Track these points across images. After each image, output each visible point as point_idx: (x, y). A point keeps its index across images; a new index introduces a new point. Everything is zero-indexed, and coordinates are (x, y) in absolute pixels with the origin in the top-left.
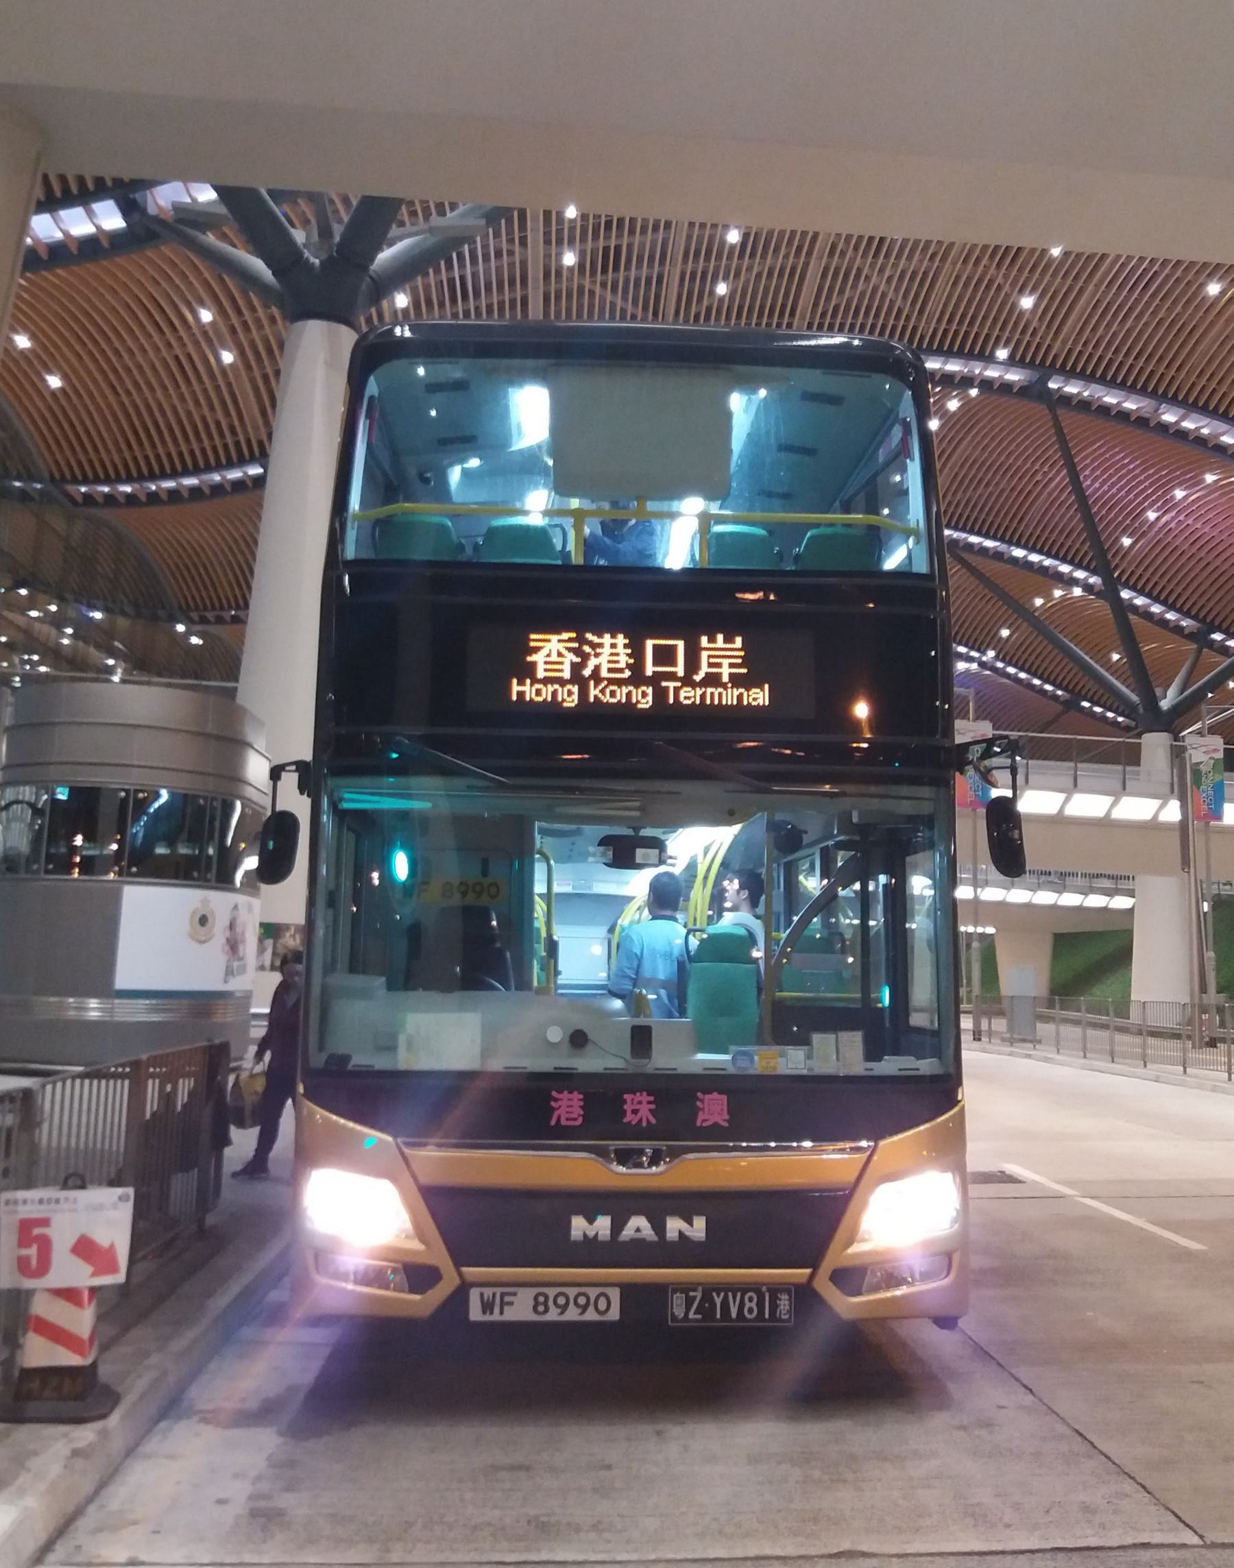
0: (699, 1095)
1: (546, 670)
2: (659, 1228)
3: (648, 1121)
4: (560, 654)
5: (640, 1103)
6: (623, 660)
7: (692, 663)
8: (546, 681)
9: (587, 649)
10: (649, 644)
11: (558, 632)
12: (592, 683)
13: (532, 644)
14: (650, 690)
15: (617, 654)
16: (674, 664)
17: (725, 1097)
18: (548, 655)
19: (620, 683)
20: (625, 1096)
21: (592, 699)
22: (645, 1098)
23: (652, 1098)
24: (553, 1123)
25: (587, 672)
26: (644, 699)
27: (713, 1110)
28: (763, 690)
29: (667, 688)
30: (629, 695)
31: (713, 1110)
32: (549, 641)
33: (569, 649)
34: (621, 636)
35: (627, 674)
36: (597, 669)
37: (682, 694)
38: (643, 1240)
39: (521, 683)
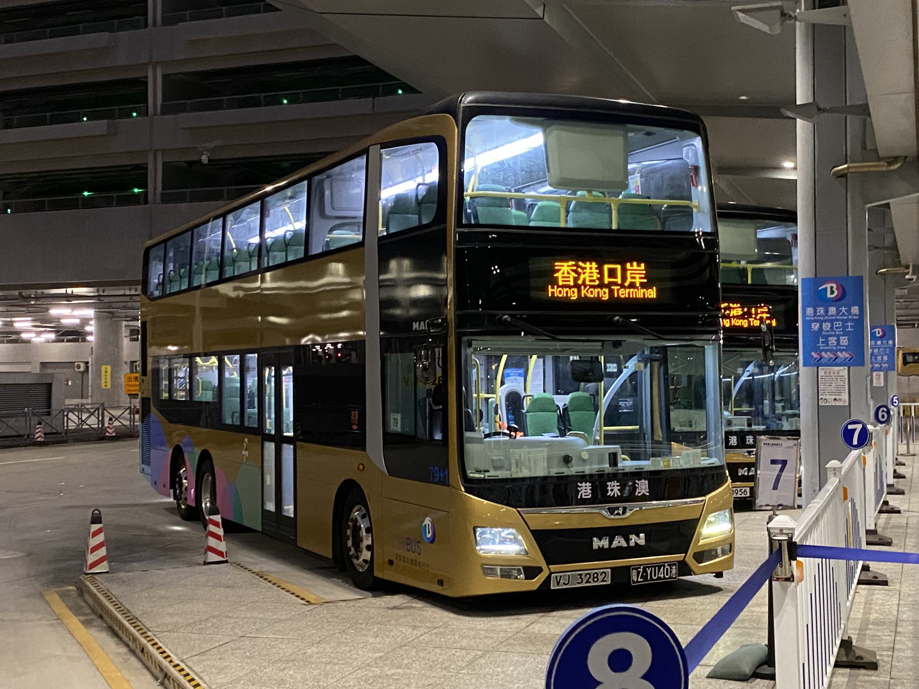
1: (563, 281)
2: (627, 540)
4: (568, 273)
6: (596, 276)
7: (624, 278)
8: (563, 286)
9: (579, 270)
10: (606, 267)
11: (567, 261)
12: (583, 287)
13: (556, 268)
14: (607, 290)
16: (616, 278)
17: (647, 482)
18: (563, 273)
20: (609, 483)
21: (583, 296)
22: (616, 484)
24: (579, 497)
25: (580, 282)
27: (643, 487)
30: (598, 293)
32: (563, 266)
33: (573, 270)
34: (594, 263)
35: (597, 283)
36: (584, 280)
37: (620, 292)
38: (621, 547)
39: (553, 288)
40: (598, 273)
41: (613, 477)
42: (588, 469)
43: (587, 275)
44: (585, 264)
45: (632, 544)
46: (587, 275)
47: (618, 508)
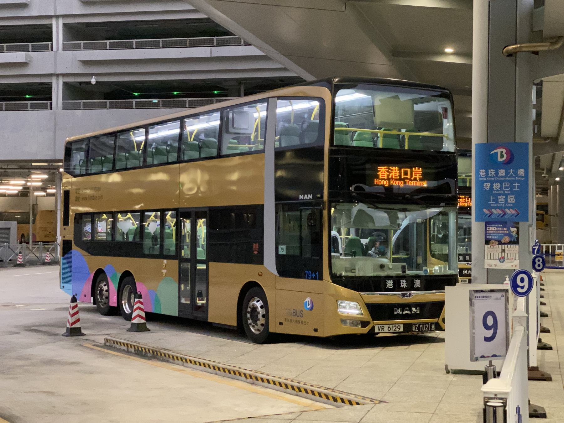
0: (415, 280)
4: (384, 172)
6: (398, 174)
7: (411, 176)
9: (390, 171)
10: (403, 169)
11: (384, 167)
14: (403, 182)
15: (396, 172)
18: (382, 173)
19: (396, 180)
25: (390, 177)
32: (381, 169)
34: (397, 168)
35: (398, 177)
36: (392, 176)
37: (409, 183)
39: (377, 180)
40: (399, 173)
41: (404, 277)
43: (393, 173)
46: (393, 173)
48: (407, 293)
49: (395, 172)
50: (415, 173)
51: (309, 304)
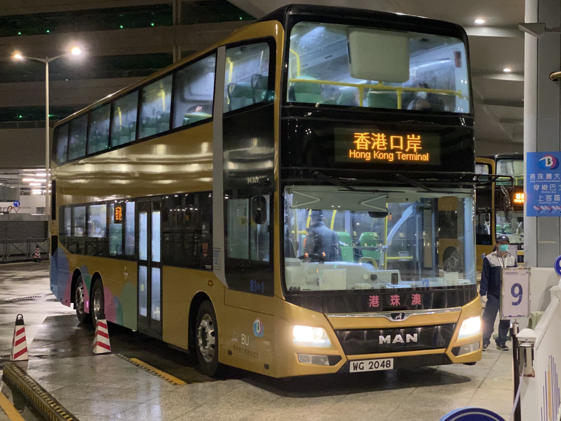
0: (413, 295)
1: (360, 146)
3: (398, 304)
4: (364, 141)
5: (395, 298)
6: (384, 143)
7: (405, 145)
8: (361, 151)
9: (372, 139)
11: (363, 132)
14: (392, 155)
15: (382, 141)
16: (399, 145)
18: (360, 141)
19: (383, 152)
20: (391, 296)
22: (397, 296)
23: (399, 297)
24: (370, 306)
25: (373, 147)
26: (391, 158)
27: (417, 299)
28: (426, 155)
29: (398, 153)
30: (386, 156)
31: (417, 299)
32: (360, 135)
33: (368, 139)
34: (383, 134)
35: (385, 148)
36: (376, 146)
38: (400, 343)
39: (353, 151)
40: (385, 141)
42: (377, 286)
43: (378, 143)
44: (377, 135)
45: (408, 341)
46: (378, 143)
47: (398, 314)
48: (398, 314)
49: (381, 141)
50: (411, 143)
51: (258, 327)
